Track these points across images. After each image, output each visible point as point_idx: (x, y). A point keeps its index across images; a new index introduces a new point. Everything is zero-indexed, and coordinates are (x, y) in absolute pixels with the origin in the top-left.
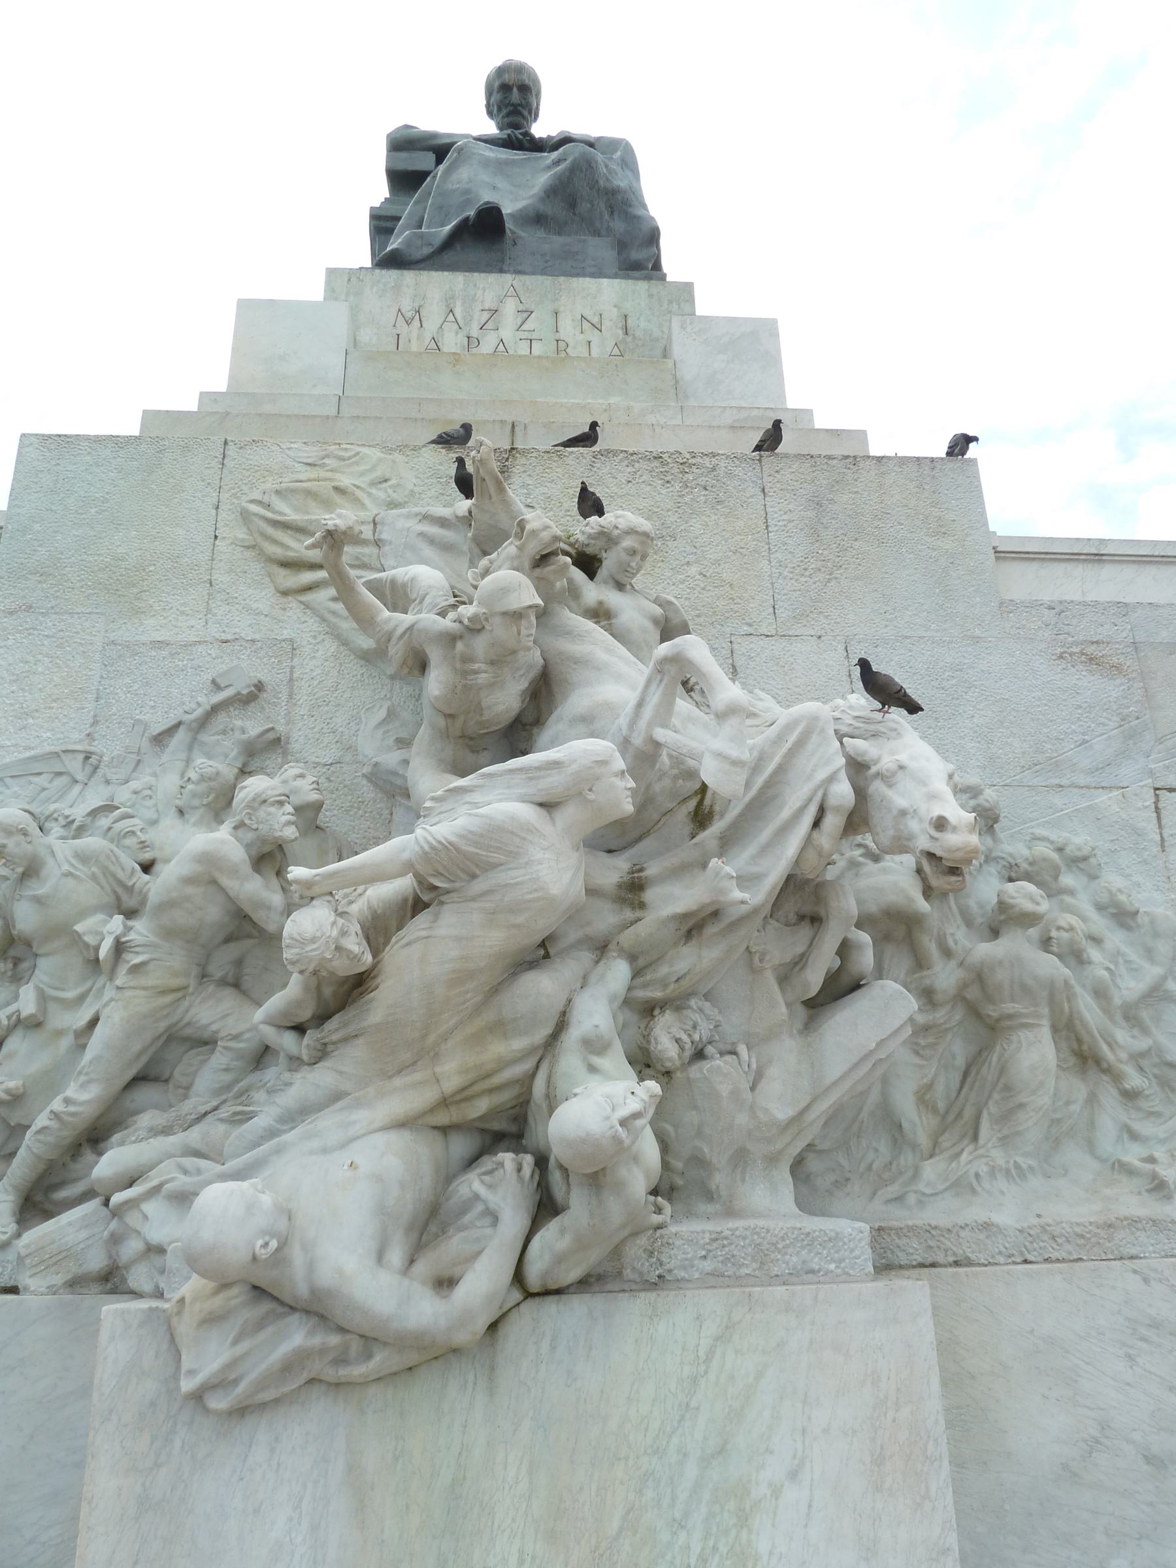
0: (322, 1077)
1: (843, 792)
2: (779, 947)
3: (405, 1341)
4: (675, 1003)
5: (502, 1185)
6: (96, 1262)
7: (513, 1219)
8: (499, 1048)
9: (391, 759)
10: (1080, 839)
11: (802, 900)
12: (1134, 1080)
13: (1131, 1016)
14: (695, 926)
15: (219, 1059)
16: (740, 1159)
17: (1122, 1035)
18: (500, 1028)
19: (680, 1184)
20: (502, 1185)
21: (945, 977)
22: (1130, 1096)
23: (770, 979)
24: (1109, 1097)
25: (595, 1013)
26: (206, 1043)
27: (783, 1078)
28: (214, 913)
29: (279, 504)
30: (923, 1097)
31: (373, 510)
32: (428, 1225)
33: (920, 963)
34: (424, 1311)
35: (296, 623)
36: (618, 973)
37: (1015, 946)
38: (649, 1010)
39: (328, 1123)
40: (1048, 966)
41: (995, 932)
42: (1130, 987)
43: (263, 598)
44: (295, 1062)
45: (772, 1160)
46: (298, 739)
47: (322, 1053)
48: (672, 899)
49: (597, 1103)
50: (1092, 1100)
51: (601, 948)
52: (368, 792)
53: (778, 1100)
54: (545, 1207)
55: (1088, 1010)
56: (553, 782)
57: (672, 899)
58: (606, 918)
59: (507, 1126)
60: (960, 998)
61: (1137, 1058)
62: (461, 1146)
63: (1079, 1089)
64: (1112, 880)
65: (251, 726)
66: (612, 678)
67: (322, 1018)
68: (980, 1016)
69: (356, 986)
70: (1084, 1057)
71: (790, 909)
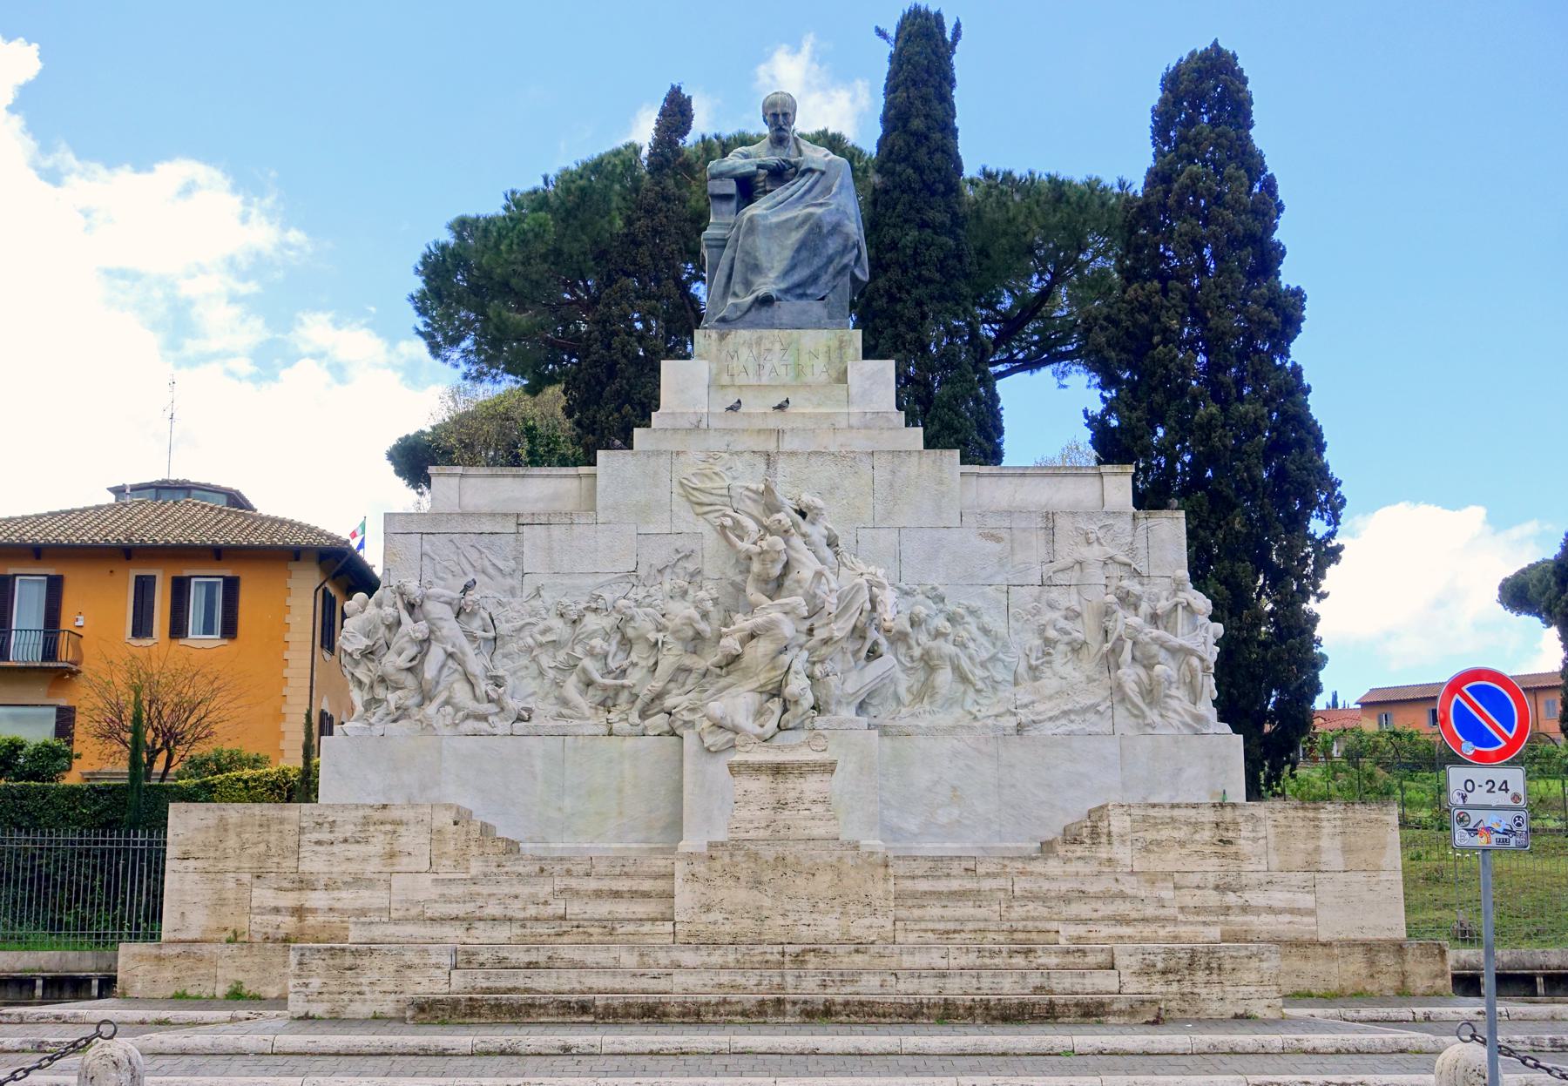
0: (729, 680)
1: (868, 606)
2: (851, 646)
4: (822, 662)
5: (776, 706)
6: (667, 728)
7: (778, 712)
8: (774, 673)
9: (738, 578)
10: (976, 603)
11: (858, 633)
12: (980, 685)
13: (983, 665)
14: (825, 642)
15: (693, 675)
16: (839, 703)
17: (979, 672)
18: (774, 668)
20: (776, 706)
21: (917, 652)
22: (978, 691)
23: (849, 655)
24: (971, 693)
27: (851, 680)
28: (691, 633)
29: (694, 480)
30: (909, 690)
31: (728, 481)
32: (760, 713)
33: (910, 647)
35: (703, 527)
36: (805, 654)
37: (940, 642)
38: (814, 663)
39: (732, 690)
41: (936, 638)
42: (985, 655)
43: (691, 517)
44: (719, 676)
45: (848, 704)
46: (710, 570)
47: (728, 674)
48: (820, 634)
49: (797, 685)
50: (965, 692)
51: (801, 647)
52: (730, 589)
53: (850, 687)
54: (785, 710)
55: (965, 664)
56: (787, 608)
57: (820, 634)
58: (803, 638)
59: (776, 692)
60: (921, 658)
61: (983, 679)
62: (765, 697)
63: (961, 688)
64: (986, 619)
65: (691, 567)
67: (728, 665)
68: (928, 663)
69: (737, 657)
70: (964, 679)
71: (856, 635)
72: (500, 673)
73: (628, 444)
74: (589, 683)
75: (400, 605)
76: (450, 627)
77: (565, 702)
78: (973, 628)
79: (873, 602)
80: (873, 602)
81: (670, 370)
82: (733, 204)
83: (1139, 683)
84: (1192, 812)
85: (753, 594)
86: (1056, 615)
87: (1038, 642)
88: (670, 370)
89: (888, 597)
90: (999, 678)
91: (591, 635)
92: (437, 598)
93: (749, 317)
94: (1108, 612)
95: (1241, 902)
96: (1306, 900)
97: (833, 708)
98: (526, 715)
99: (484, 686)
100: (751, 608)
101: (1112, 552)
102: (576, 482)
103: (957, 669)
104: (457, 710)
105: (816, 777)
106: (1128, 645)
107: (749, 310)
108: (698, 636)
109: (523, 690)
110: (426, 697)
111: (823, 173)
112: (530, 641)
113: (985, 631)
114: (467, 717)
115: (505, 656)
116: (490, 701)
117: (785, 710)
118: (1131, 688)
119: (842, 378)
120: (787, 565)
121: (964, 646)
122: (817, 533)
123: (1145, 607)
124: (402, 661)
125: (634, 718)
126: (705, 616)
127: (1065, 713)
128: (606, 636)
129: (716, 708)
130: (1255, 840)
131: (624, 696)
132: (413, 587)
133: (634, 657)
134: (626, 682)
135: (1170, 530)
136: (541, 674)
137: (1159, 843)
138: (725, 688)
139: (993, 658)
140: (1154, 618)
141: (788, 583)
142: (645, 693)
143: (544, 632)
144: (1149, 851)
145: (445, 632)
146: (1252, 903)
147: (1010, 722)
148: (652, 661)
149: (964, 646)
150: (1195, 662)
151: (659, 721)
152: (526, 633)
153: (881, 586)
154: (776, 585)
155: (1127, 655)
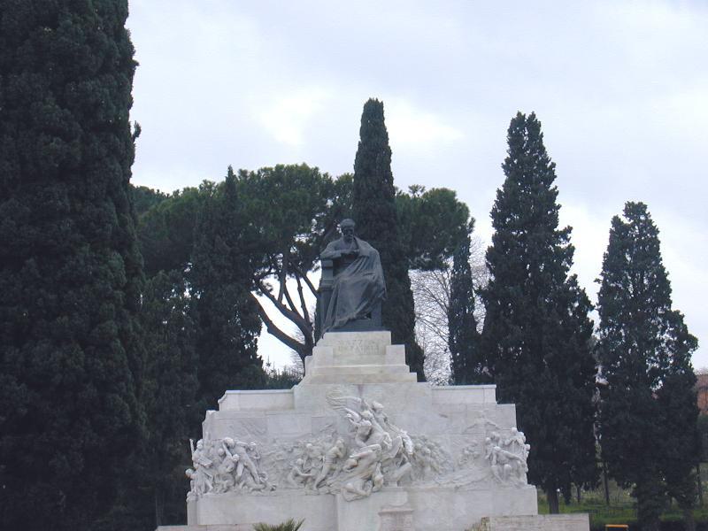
0: (352, 474)
2: (395, 460)
11: (398, 456)
12: (441, 472)
13: (442, 464)
15: (336, 472)
17: (440, 467)
19: (386, 484)
20: (370, 483)
25: (378, 469)
26: (334, 470)
34: (363, 492)
40: (429, 459)
49: (379, 477)
54: (374, 485)
55: (435, 464)
59: (370, 478)
61: (442, 470)
64: (442, 447)
65: (333, 430)
66: (380, 433)
68: (423, 466)
72: (264, 472)
74: (297, 475)
75: (224, 446)
76: (246, 456)
77: (287, 482)
79: (404, 444)
80: (404, 444)
82: (331, 272)
83: (499, 470)
85: (359, 442)
86: (468, 445)
87: (461, 455)
89: (410, 443)
90: (447, 468)
91: (297, 457)
92: (240, 445)
94: (487, 444)
99: (258, 478)
100: (359, 447)
102: (283, 395)
103: (432, 467)
104: (249, 487)
106: (495, 457)
107: (347, 323)
108: (338, 457)
109: (272, 479)
110: (237, 482)
111: (368, 257)
112: (273, 460)
113: (442, 452)
114: (254, 490)
115: (264, 465)
116: (261, 483)
117: (374, 485)
118: (496, 473)
119: (384, 352)
120: (371, 431)
121: (434, 458)
122: (381, 417)
123: (500, 442)
124: (228, 470)
125: (315, 488)
126: (340, 449)
128: (302, 458)
129: (350, 485)
131: (309, 480)
132: (230, 441)
133: (313, 465)
134: (311, 474)
135: (510, 409)
136: (278, 472)
138: (350, 478)
139: (445, 462)
140: (504, 446)
141: (372, 437)
142: (318, 479)
143: (278, 456)
145: (244, 458)
147: (454, 486)
148: (319, 467)
149: (434, 458)
150: (519, 462)
151: (325, 489)
153: (406, 438)
154: (366, 438)
155: (494, 461)
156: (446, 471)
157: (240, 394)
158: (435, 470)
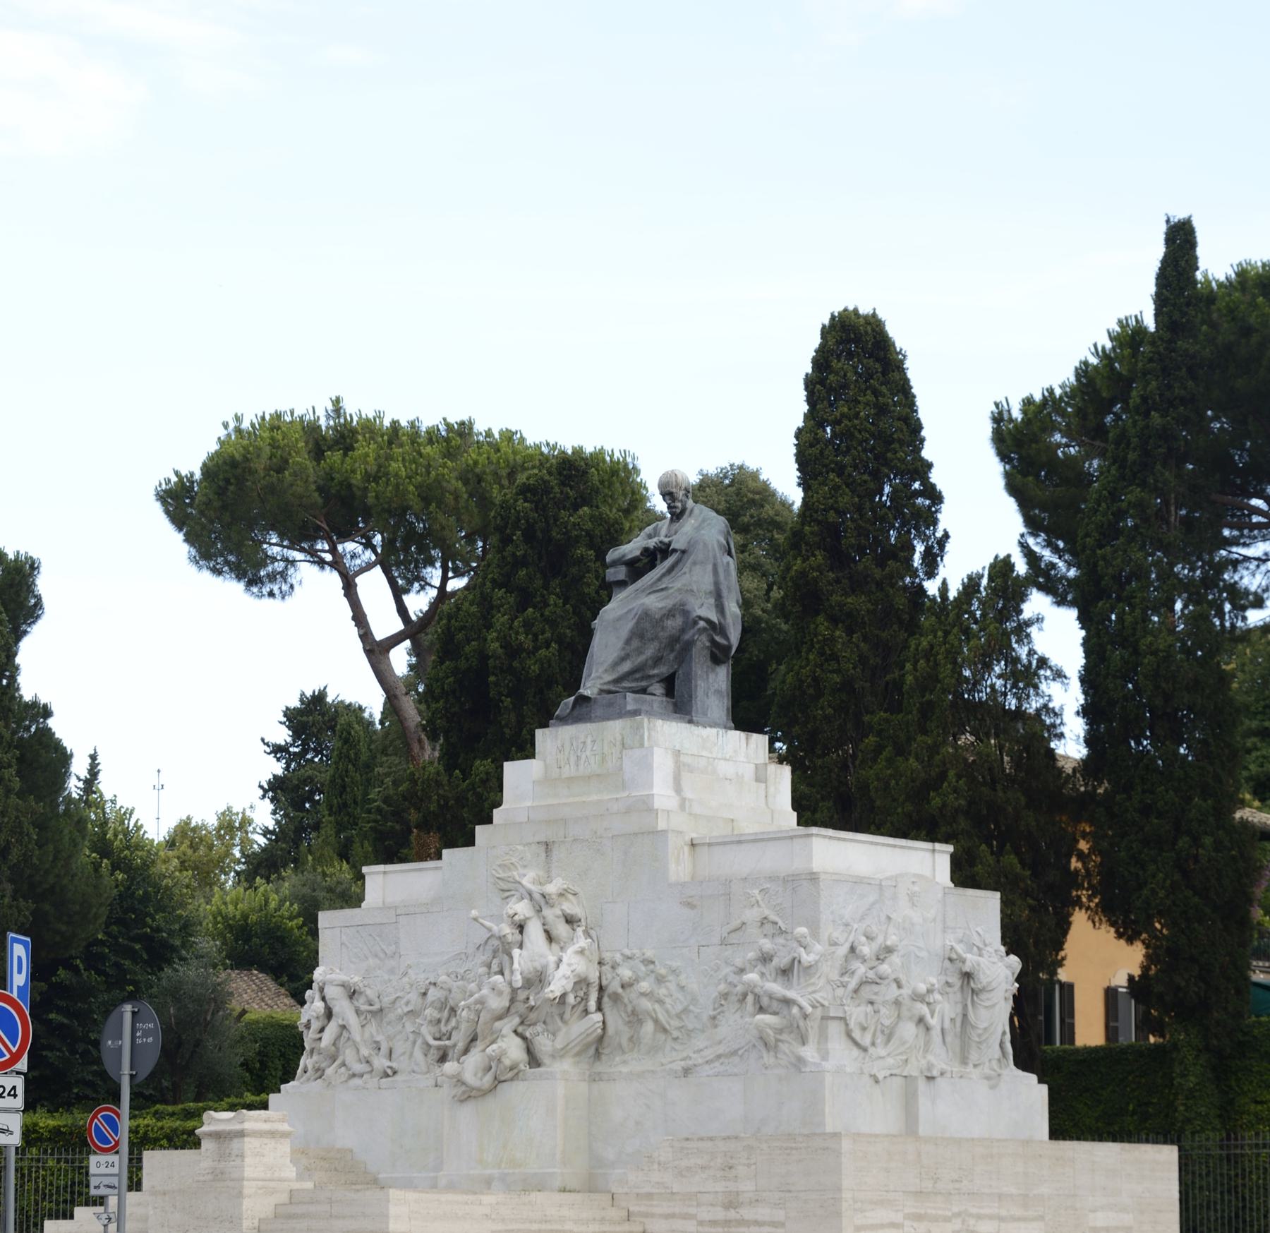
3: (479, 1090)
12: (676, 1034)
17: (675, 1023)
21: (629, 1009)
22: (676, 1039)
42: (679, 1008)
55: (662, 1018)
61: (679, 1028)
63: (662, 1037)
73: (470, 841)
78: (672, 986)
81: (512, 770)
84: (710, 1144)
88: (512, 770)
90: (690, 1026)
93: (575, 713)
95: (738, 1217)
96: (780, 1215)
97: (546, 1060)
98: (389, 1072)
101: (767, 912)
105: (236, 1140)
111: (684, 552)
115: (389, 1023)
127: (719, 1057)
130: (749, 1165)
137: (688, 1169)
139: (686, 1010)
144: (682, 1176)
146: (746, 1217)
152: (398, 1004)
156: (689, 1033)
157: (385, 873)
158: (665, 1030)
